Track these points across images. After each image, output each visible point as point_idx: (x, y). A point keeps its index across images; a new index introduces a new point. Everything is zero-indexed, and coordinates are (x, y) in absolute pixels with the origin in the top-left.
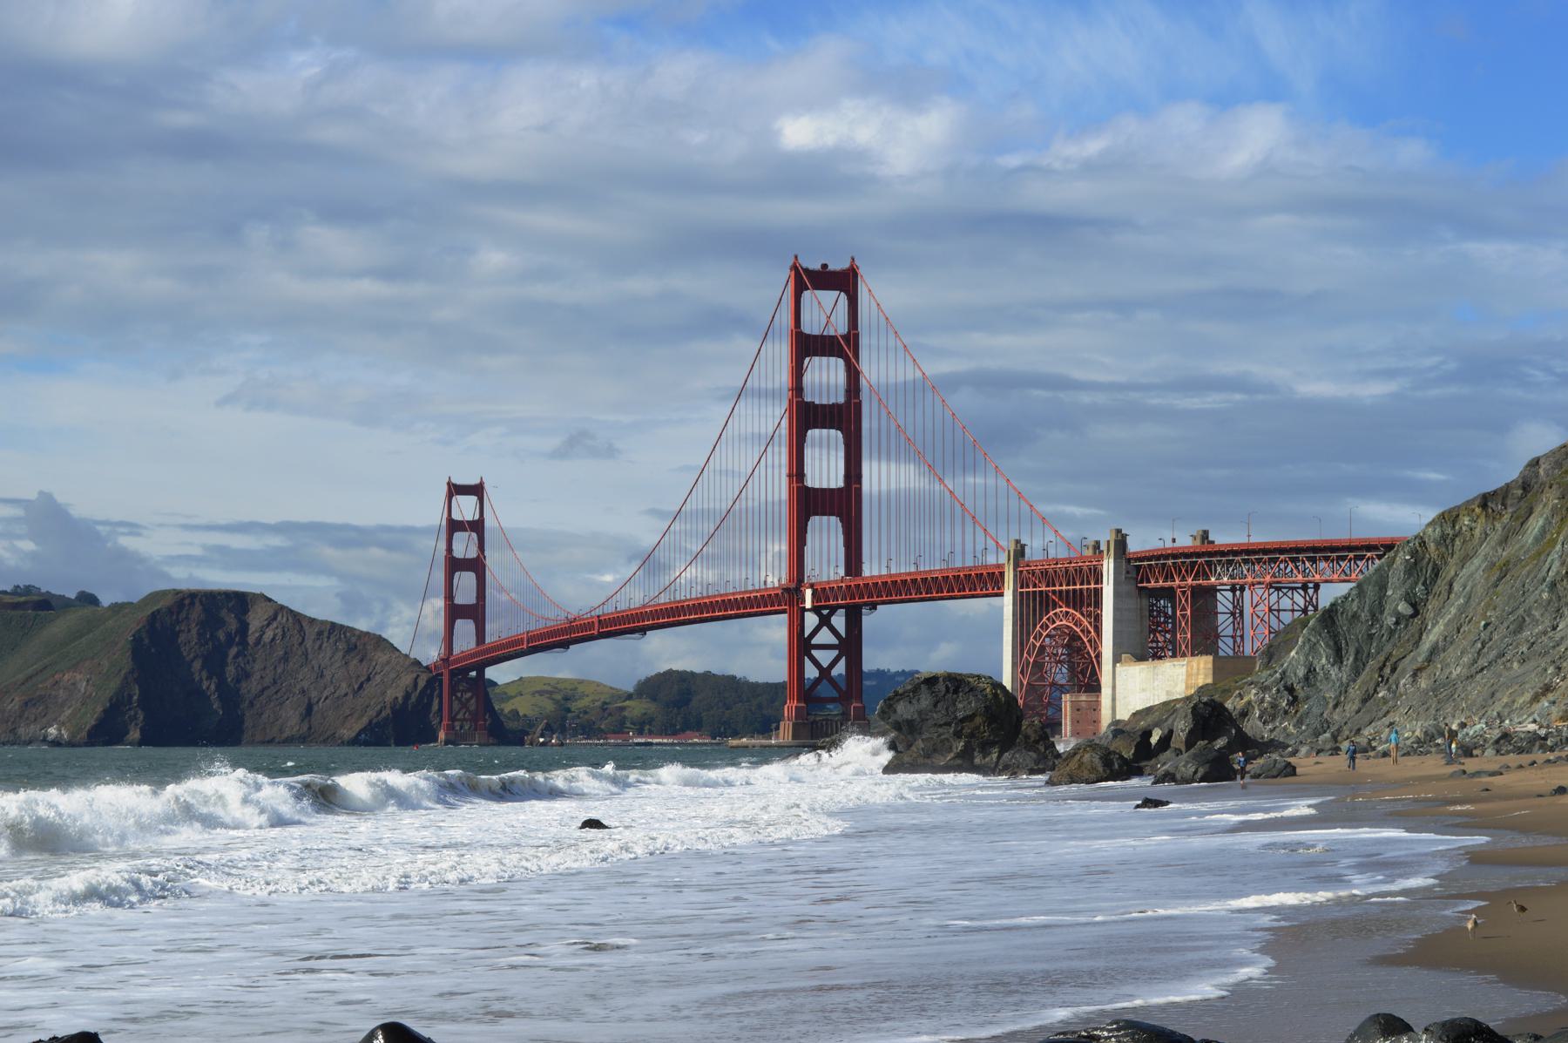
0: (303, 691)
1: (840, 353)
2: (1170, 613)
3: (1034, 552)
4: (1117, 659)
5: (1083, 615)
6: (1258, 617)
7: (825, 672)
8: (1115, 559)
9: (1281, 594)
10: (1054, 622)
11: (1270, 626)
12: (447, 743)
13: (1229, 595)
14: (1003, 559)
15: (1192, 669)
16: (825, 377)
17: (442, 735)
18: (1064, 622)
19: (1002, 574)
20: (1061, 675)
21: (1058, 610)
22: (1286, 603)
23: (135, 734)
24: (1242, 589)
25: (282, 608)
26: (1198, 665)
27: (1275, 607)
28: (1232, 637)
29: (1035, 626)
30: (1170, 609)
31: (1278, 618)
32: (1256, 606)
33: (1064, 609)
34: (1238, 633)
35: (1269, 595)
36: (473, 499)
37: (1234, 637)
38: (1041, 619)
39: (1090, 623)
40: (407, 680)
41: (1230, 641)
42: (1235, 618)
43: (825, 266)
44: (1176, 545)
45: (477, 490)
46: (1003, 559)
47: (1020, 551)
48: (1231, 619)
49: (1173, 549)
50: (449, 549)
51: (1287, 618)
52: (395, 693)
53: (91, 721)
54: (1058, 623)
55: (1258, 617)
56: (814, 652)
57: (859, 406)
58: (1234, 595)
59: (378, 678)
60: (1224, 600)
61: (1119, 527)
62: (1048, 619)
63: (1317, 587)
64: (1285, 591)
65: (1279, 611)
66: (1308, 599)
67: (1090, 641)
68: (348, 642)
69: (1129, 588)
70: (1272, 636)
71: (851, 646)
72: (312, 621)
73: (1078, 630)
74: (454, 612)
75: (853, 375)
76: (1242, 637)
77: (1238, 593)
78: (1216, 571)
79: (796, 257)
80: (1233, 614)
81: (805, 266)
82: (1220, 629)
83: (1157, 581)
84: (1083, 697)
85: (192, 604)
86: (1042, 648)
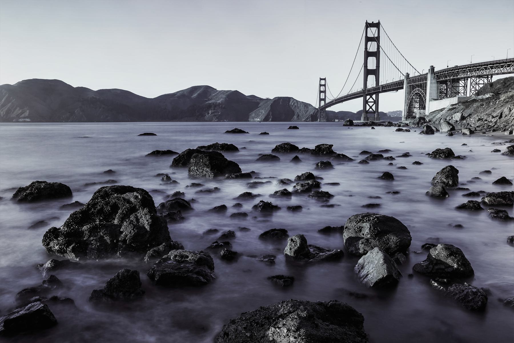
0: (297, 113)
1: (375, 41)
2: (446, 88)
3: (411, 76)
4: (430, 100)
5: (422, 90)
6: (472, 86)
7: (371, 107)
8: (431, 74)
9: (480, 79)
10: (415, 92)
11: (476, 89)
12: (319, 121)
13: (463, 81)
14: (404, 78)
15: (451, 101)
16: (372, 47)
17: (319, 120)
18: (417, 92)
19: (404, 82)
20: (417, 105)
21: (416, 89)
22: (481, 82)
23: (270, 120)
24: (467, 80)
25: (295, 99)
26: (453, 100)
27: (478, 83)
28: (463, 93)
29: (410, 94)
30: (446, 87)
31: (479, 86)
32: (472, 83)
33: (418, 88)
34: (465, 92)
35: (476, 79)
36: (324, 81)
37: (464, 93)
38: (412, 91)
39: (424, 91)
40: (314, 111)
41: (463, 94)
42: (464, 88)
43: (373, 22)
44: (448, 68)
45: (325, 79)
46: (404, 78)
47: (408, 75)
48: (463, 88)
49: (447, 69)
50: (320, 89)
51: (481, 86)
52: (312, 113)
53: (263, 118)
54: (416, 92)
55: (472, 86)
56: (368, 103)
57: (379, 51)
58: (465, 82)
59: (309, 111)
60: (462, 83)
61: (432, 65)
62: (414, 91)
63: (492, 77)
64: (481, 78)
65: (479, 84)
66: (488, 80)
67: (423, 96)
68: (305, 105)
69: (434, 81)
70: (477, 91)
71: (376, 102)
72: (299, 101)
73: (421, 93)
74: (321, 100)
75: (378, 47)
76: (466, 93)
77: (466, 81)
78: (460, 73)
79: (367, 21)
80: (464, 87)
81: (368, 22)
82: (460, 91)
83: (442, 79)
84: (422, 111)
85: (281, 99)
86: (412, 98)
